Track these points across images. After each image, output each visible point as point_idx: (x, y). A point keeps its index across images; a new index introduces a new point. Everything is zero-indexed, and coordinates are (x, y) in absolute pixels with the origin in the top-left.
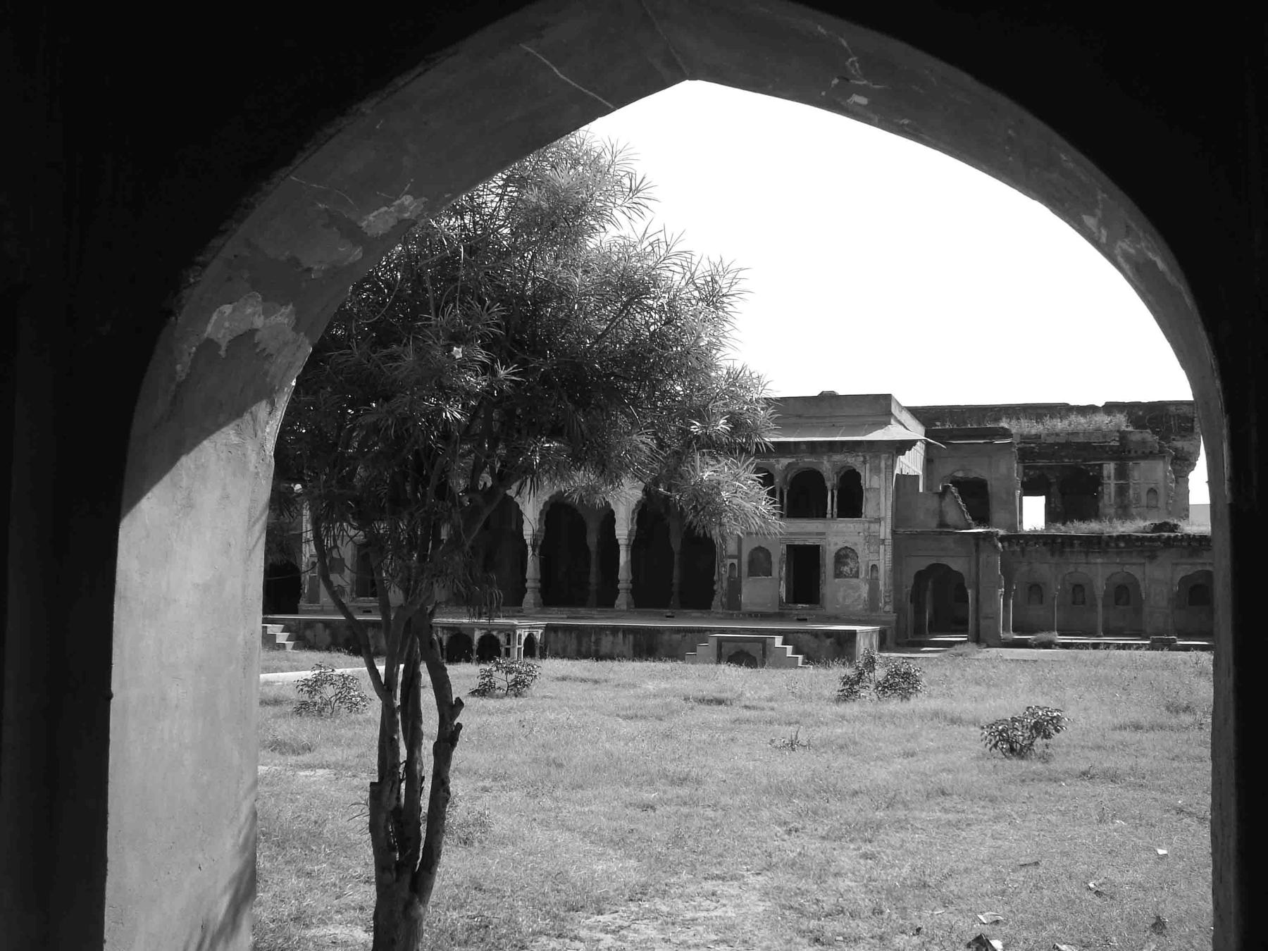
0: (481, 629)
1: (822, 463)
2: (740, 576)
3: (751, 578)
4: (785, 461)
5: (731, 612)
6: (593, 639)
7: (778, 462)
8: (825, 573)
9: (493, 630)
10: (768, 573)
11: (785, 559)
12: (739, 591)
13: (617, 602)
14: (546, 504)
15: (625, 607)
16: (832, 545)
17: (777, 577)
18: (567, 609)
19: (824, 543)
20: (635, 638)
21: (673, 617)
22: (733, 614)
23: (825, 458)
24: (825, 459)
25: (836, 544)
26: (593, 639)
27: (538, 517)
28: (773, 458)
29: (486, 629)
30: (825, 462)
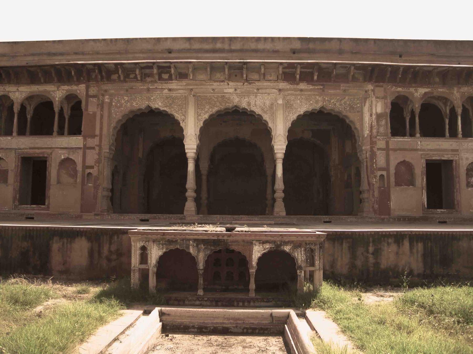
0: (264, 242)
1: (453, 93)
2: (389, 187)
3: (398, 188)
4: (422, 91)
5: (382, 217)
6: (371, 249)
7: (416, 91)
8: (459, 182)
9: (286, 243)
10: (411, 183)
11: (425, 172)
12: (389, 199)
13: (276, 209)
14: (206, 123)
15: (284, 213)
16: (464, 159)
17: (420, 186)
18: (230, 216)
19: (457, 158)
20: (425, 248)
21: (329, 222)
22: (384, 218)
23: (456, 89)
24: (455, 90)
25: (467, 159)
26: (371, 249)
27: (198, 133)
28: (413, 87)
29: (274, 242)
30: (455, 92)
